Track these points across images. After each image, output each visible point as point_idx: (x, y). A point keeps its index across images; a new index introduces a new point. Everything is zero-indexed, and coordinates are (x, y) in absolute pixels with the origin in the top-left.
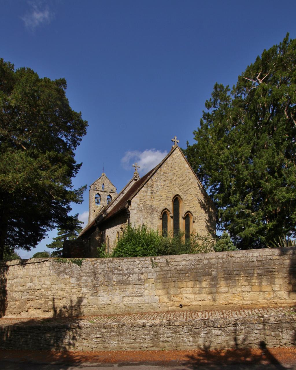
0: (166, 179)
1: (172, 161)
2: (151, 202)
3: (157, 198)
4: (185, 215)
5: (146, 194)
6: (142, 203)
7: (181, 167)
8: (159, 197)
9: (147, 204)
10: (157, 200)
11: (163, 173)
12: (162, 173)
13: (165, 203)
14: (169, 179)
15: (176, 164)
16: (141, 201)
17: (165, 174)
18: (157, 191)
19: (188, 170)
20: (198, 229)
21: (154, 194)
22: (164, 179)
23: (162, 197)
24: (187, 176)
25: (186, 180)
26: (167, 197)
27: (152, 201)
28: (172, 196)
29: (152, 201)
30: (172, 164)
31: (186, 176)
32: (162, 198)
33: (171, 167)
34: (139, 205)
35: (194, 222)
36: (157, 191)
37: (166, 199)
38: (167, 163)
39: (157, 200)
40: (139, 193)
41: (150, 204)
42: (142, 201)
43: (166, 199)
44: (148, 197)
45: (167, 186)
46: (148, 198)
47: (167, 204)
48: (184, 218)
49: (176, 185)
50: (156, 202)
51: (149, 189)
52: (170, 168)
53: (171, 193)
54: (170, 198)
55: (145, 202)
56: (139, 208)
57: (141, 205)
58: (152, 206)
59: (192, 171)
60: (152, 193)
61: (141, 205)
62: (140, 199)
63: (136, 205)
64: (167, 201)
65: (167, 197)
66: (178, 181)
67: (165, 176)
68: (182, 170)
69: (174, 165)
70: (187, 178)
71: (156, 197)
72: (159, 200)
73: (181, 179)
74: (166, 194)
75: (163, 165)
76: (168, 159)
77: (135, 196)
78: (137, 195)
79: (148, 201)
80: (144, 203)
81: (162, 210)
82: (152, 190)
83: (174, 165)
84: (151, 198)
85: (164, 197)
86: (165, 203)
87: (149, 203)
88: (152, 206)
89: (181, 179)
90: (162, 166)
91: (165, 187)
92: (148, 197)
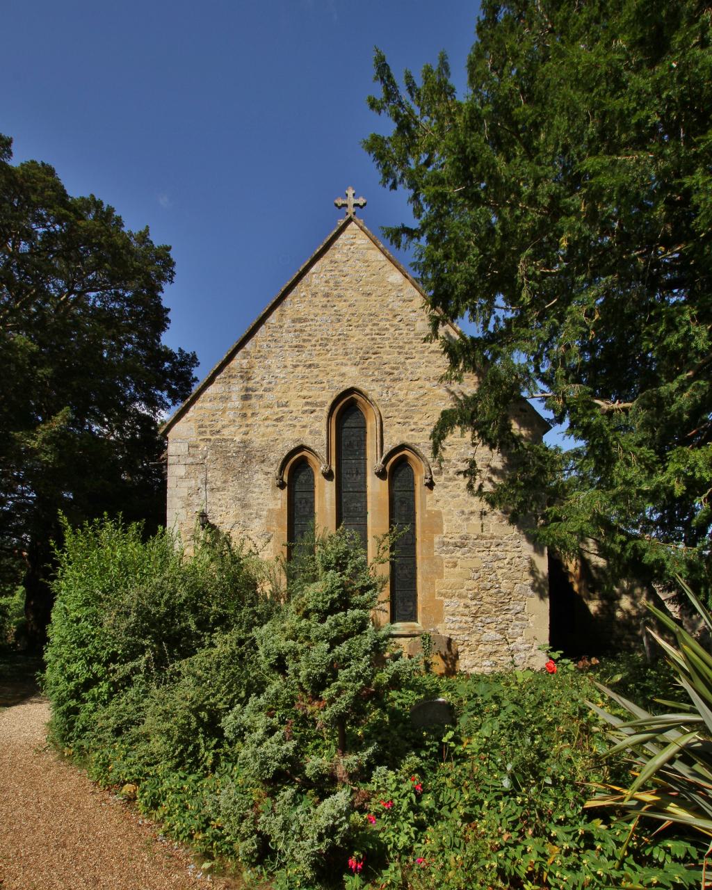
0: (304, 341)
1: (328, 274)
2: (244, 429)
3: (268, 412)
4: (385, 462)
5: (221, 406)
6: (210, 440)
7: (367, 289)
8: (276, 409)
9: (225, 440)
10: (266, 419)
11: (293, 321)
12: (287, 322)
13: (298, 428)
14: (319, 336)
15: (347, 279)
16: (201, 433)
17: (298, 326)
18: (265, 390)
19: (401, 290)
20: (450, 512)
21: (253, 401)
22: (295, 343)
23: (286, 406)
24: (395, 316)
25: (392, 330)
26: (307, 403)
27: (247, 426)
28: (328, 397)
29: (247, 426)
30: (331, 284)
31: (390, 317)
32: (286, 409)
33: (327, 295)
34: (197, 447)
35: (431, 485)
36: (265, 390)
37: (305, 412)
38: (309, 286)
39: (266, 419)
40: (198, 404)
41: (237, 439)
42: (208, 430)
43: (305, 412)
44: (230, 415)
45: (310, 366)
46: (231, 417)
47: (308, 430)
48: (381, 475)
49: (346, 354)
50: (262, 429)
51: (237, 387)
52: (320, 300)
53: (324, 389)
54: (322, 404)
55: (219, 432)
56: (193, 456)
57: (203, 446)
58: (245, 444)
59: (417, 293)
60: (246, 398)
61: (202, 444)
62: (201, 426)
63: (183, 448)
64: (307, 419)
65: (307, 403)
66: (358, 338)
67: (301, 331)
68: (373, 297)
69: (337, 284)
70: (395, 322)
71: (262, 411)
72: (277, 420)
73: (367, 331)
74: (304, 393)
75: (292, 295)
76: (313, 270)
77: (183, 419)
78: (188, 415)
79: (233, 429)
80: (212, 438)
81: (286, 453)
82: (247, 389)
83: (337, 284)
84: (245, 416)
85: (297, 405)
86: (298, 428)
87: (234, 434)
88: (245, 444)
89: (367, 331)
90: (288, 299)
91: (299, 369)
92: (230, 415)
